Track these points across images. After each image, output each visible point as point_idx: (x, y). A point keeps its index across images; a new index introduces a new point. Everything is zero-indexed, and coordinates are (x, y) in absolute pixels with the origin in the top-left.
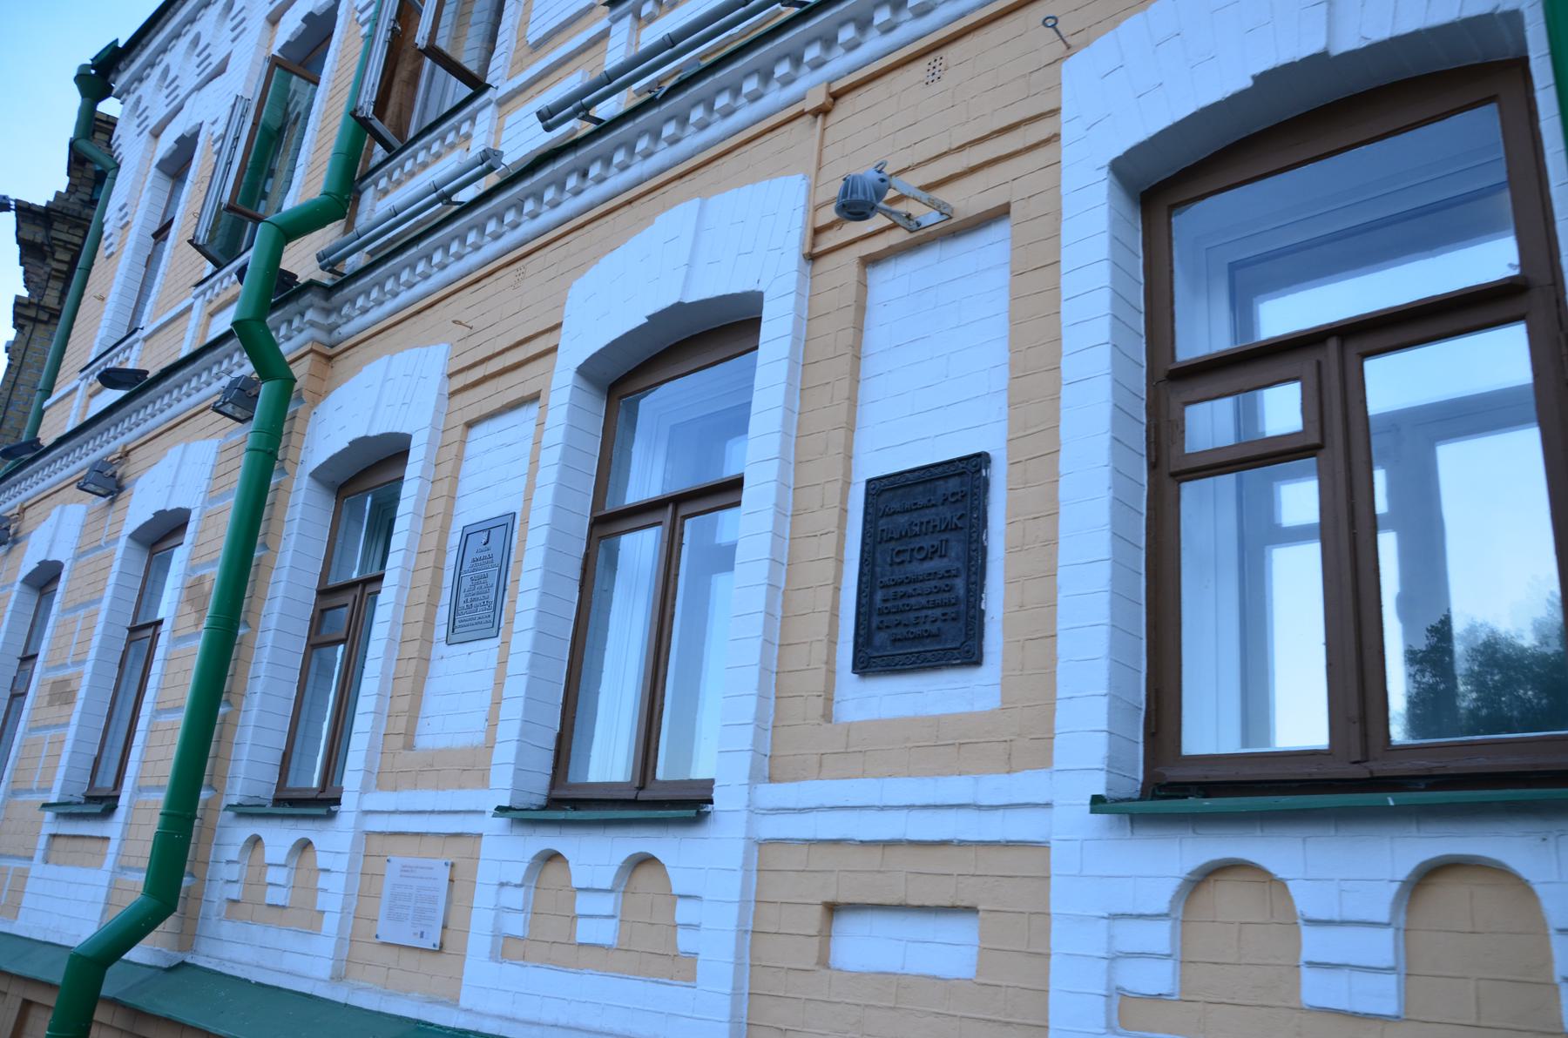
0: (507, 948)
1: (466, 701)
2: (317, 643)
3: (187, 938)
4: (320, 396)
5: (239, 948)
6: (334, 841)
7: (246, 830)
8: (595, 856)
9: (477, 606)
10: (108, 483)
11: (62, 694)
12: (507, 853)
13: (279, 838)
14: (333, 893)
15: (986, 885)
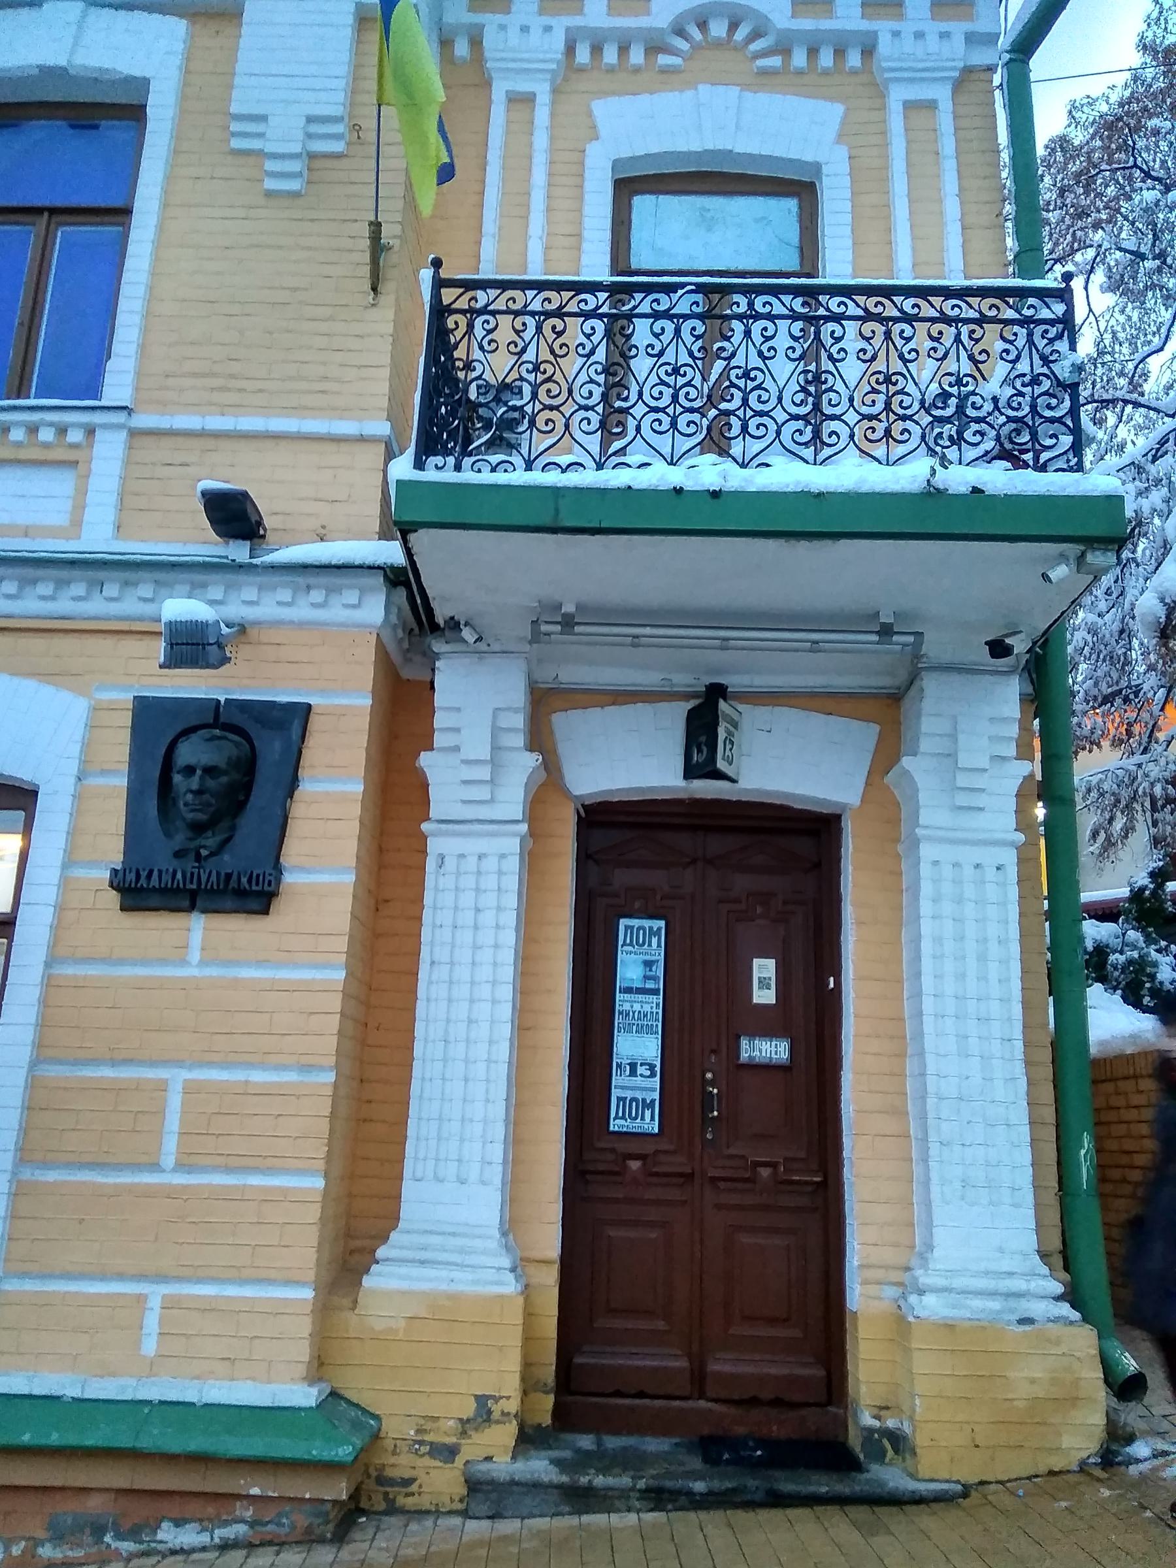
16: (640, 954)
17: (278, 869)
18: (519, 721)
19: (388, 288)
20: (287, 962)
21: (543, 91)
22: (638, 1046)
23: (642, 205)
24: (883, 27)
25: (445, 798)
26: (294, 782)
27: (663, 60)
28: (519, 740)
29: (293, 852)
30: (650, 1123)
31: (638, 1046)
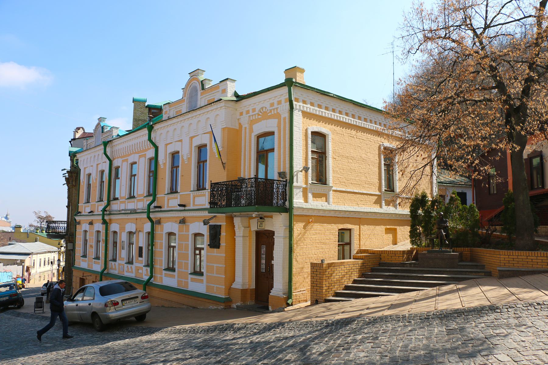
0: (126, 272)
1: (123, 254)
2: (114, 246)
3: (108, 270)
4: (110, 224)
5: (112, 272)
6: (117, 263)
7: (111, 262)
8: (129, 266)
9: (123, 248)
10: (91, 223)
11: (91, 246)
12: (126, 265)
13: (113, 263)
14: (117, 267)
15: (141, 268)
16: (263, 250)
17: (220, 244)
18: (240, 224)
19: (226, 169)
20: (220, 254)
21: (247, 126)
22: (263, 261)
23: (260, 139)
24: (279, 106)
25: (237, 234)
26: (220, 234)
27: (259, 117)
28: (241, 226)
29: (221, 242)
30: (264, 271)
31: (263, 261)
